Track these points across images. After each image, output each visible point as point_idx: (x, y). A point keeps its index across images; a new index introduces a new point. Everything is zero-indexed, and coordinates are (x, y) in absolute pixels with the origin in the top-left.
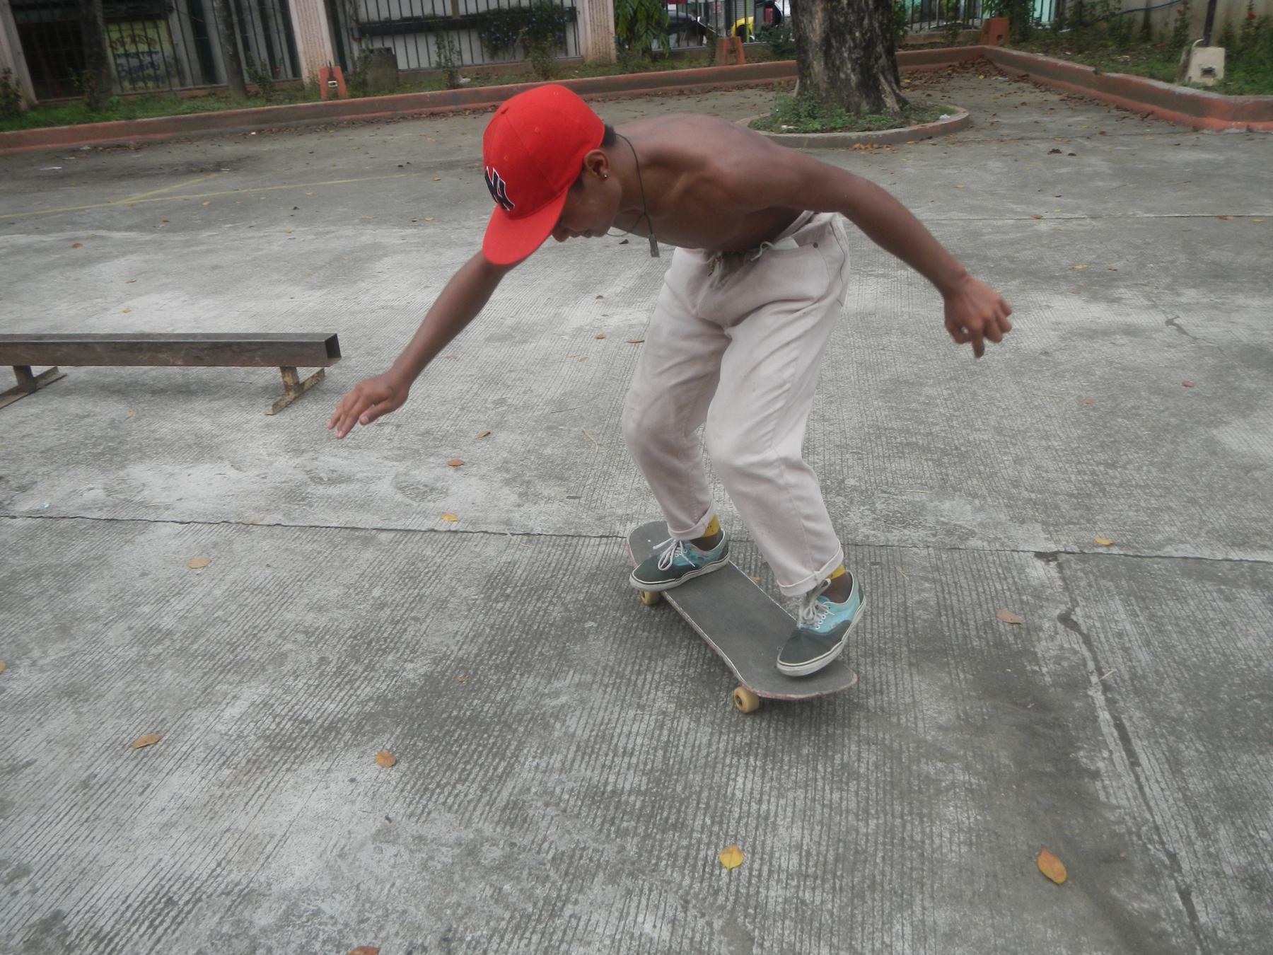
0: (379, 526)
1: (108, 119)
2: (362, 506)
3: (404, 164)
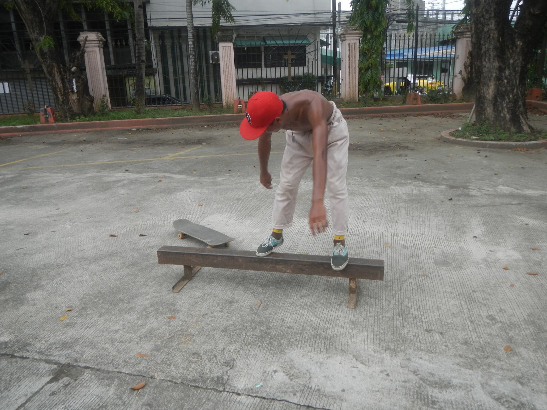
1: (145, 118)
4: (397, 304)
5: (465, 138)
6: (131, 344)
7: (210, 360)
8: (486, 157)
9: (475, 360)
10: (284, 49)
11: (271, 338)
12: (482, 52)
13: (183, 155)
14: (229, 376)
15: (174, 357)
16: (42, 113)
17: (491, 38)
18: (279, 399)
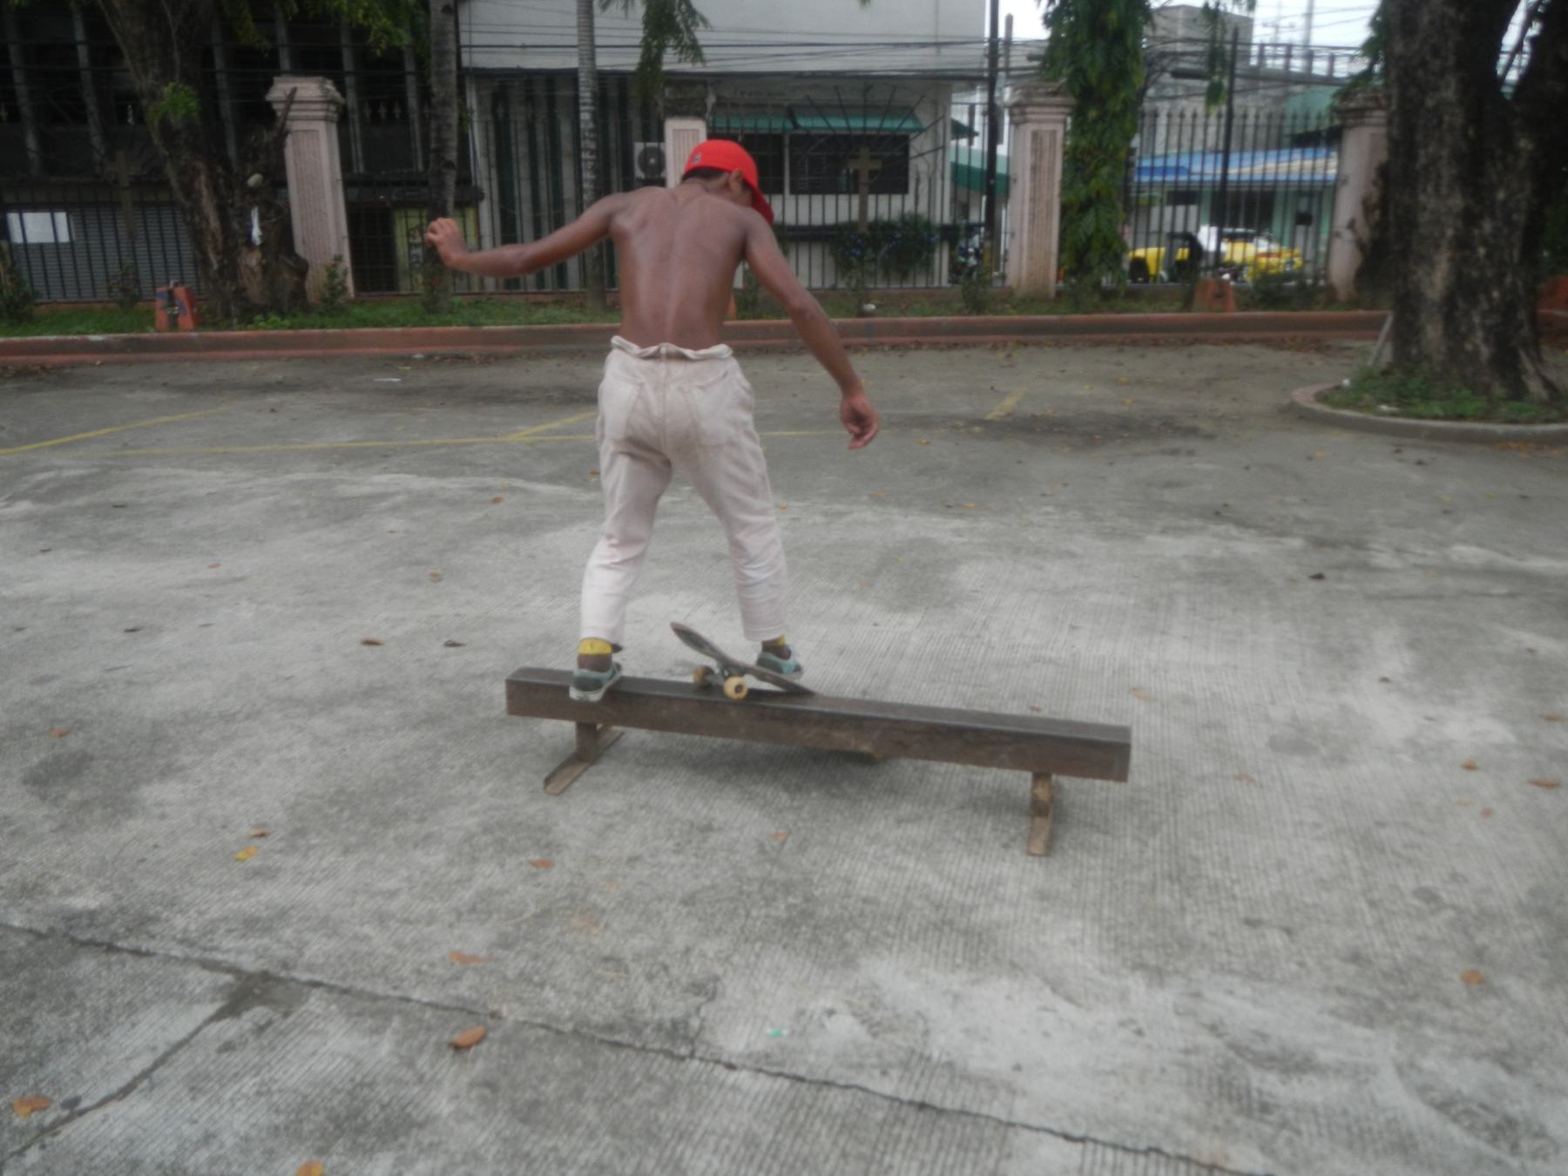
1: (449, 324)
4: (1166, 848)
5: (1360, 409)
6: (433, 928)
7: (650, 977)
8: (1420, 463)
9: (1380, 1005)
10: (845, 144)
12: (1418, 166)
13: (558, 432)
14: (703, 1020)
15: (551, 965)
16: (160, 303)
17: (1445, 126)
18: (842, 1082)
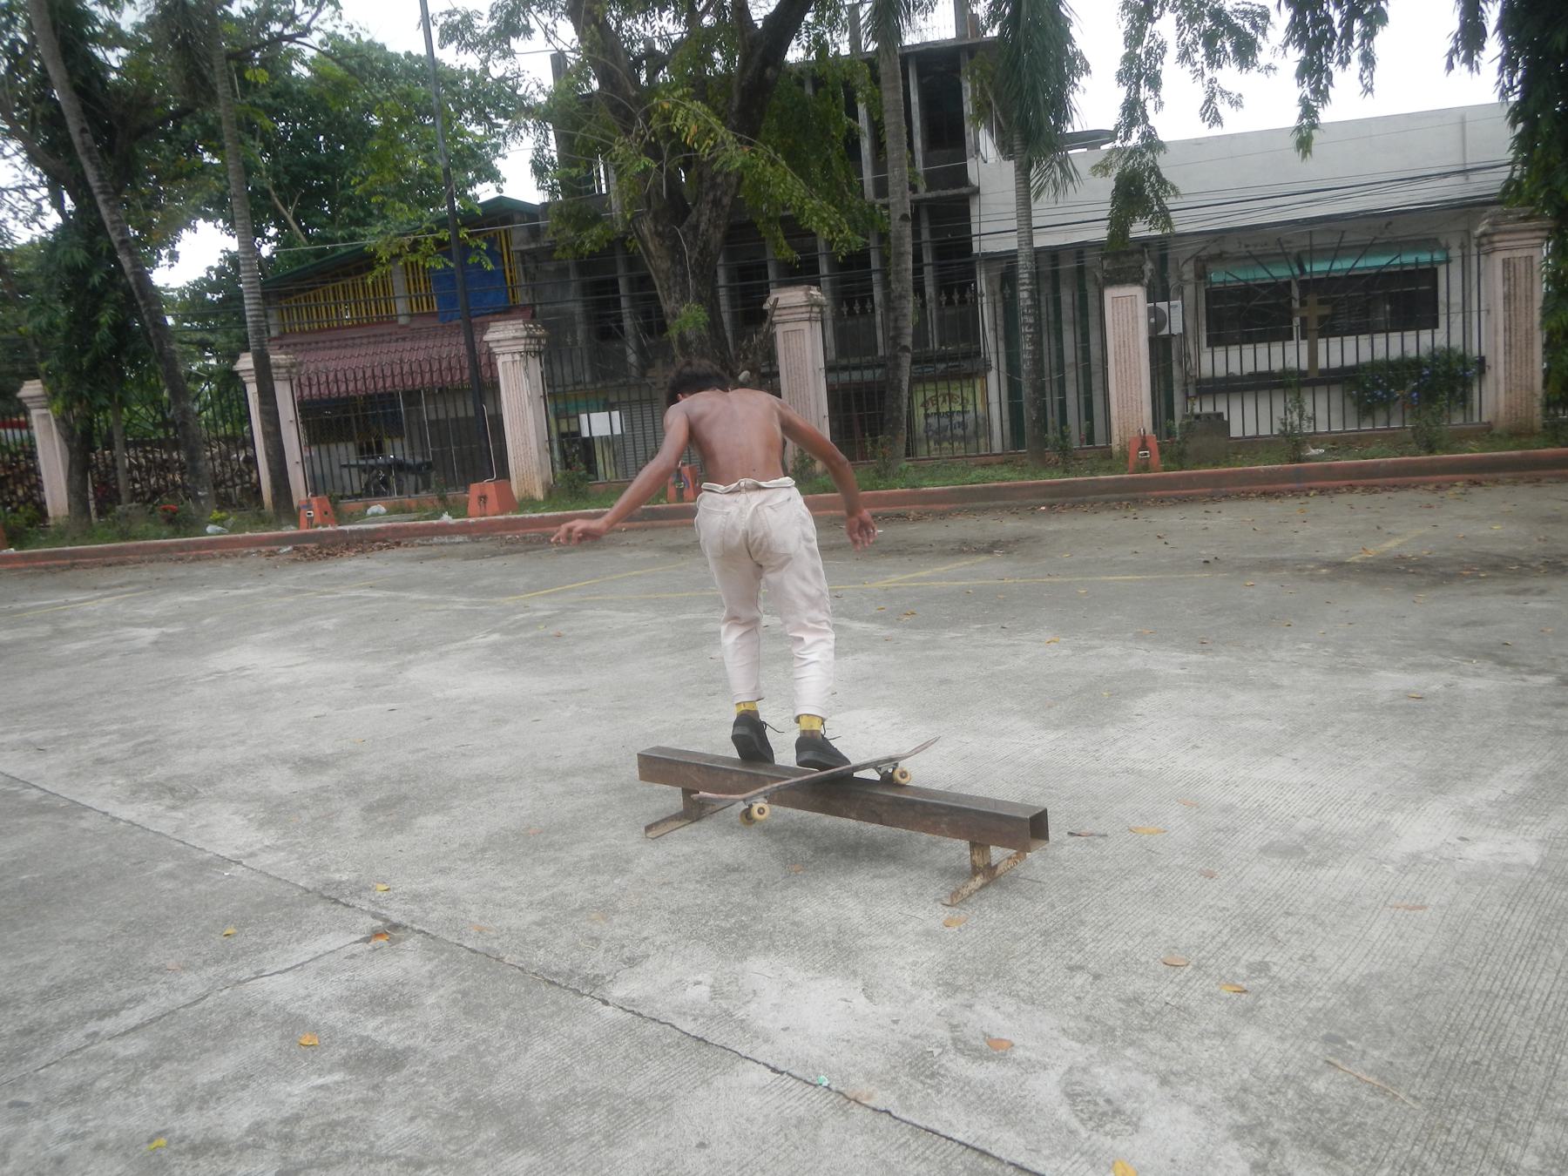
0: (1020, 1160)
2: (1006, 1113)
3: (1211, 559)
11: (743, 936)
